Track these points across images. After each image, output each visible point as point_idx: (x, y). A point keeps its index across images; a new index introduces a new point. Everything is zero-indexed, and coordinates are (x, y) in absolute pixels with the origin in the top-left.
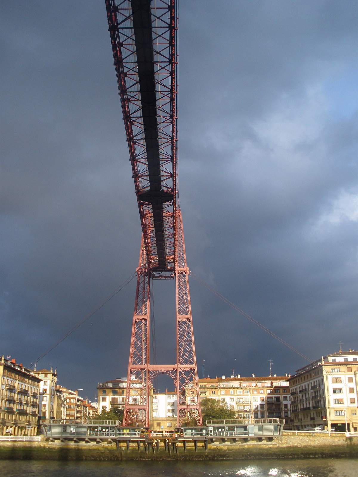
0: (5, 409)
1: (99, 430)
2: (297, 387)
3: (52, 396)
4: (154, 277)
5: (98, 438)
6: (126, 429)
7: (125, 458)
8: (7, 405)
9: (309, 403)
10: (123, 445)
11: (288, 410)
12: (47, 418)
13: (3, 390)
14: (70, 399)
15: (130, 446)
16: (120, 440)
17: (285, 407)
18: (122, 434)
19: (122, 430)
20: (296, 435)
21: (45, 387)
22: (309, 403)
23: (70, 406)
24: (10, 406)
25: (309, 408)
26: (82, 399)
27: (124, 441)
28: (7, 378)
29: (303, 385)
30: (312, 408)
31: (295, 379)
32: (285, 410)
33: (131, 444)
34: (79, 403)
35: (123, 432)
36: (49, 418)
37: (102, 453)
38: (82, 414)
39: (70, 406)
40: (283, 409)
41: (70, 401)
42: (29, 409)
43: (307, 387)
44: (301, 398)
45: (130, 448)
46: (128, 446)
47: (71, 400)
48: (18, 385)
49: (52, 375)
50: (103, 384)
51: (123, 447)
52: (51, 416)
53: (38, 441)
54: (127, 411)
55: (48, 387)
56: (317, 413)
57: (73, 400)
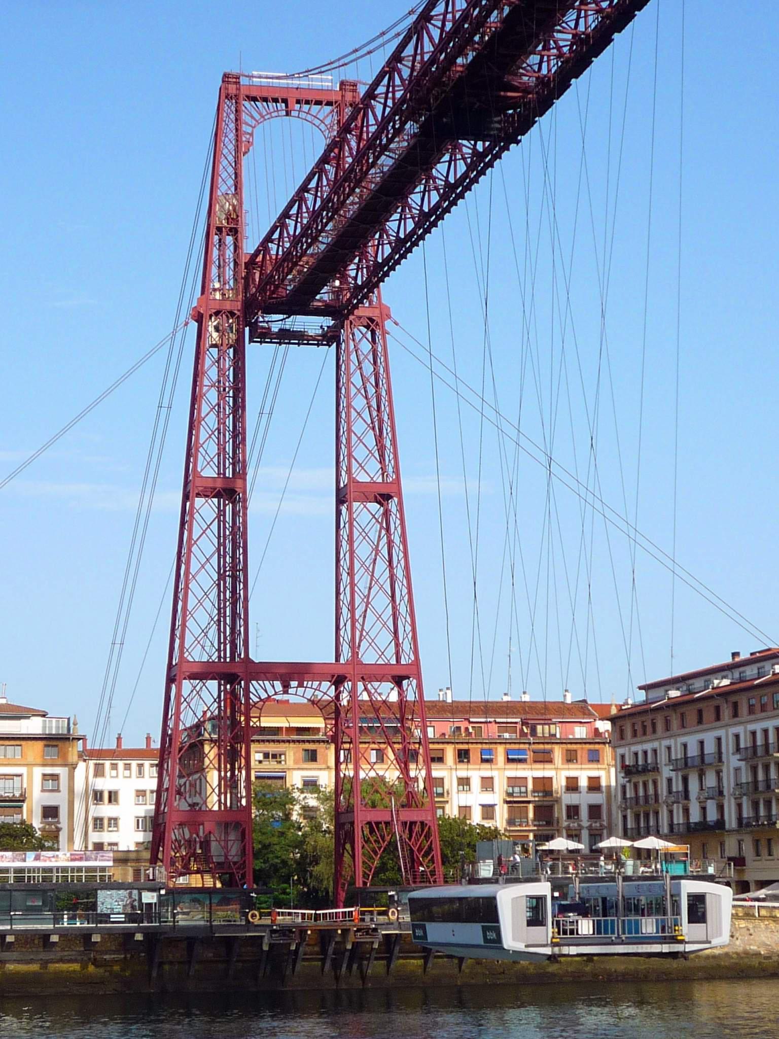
2: (656, 744)
4: (263, 335)
9: (721, 808)
11: (580, 828)
17: (569, 817)
20: (754, 916)
22: (721, 808)
25: (720, 824)
29: (692, 741)
30: (731, 821)
31: (648, 719)
32: (591, 825)
40: (565, 824)
43: (710, 748)
44: (678, 786)
56: (757, 843)
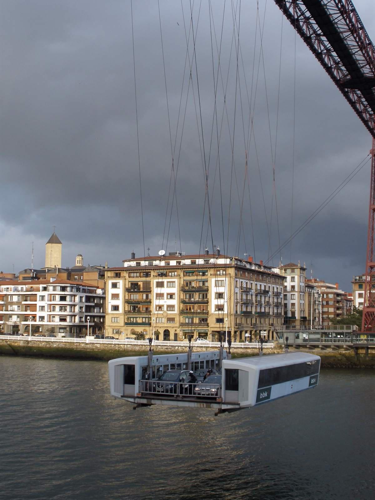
0: (241, 313)
1: (333, 336)
3: (301, 293)
5: (332, 344)
6: (364, 334)
7: (364, 366)
8: (244, 309)
10: (362, 352)
12: (297, 318)
13: (237, 293)
14: (327, 294)
15: (369, 352)
16: (358, 347)
18: (359, 341)
19: (359, 335)
21: (293, 284)
23: (327, 303)
24: (248, 310)
26: (343, 293)
27: (362, 348)
28: (241, 280)
33: (370, 351)
34: (339, 298)
35: (360, 338)
36: (299, 318)
37: (339, 360)
38: (345, 310)
39: (327, 303)
41: (328, 297)
42: (272, 311)
45: (369, 355)
46: (367, 353)
47: (329, 295)
48: (257, 285)
49: (299, 269)
50: (359, 277)
51: (362, 354)
52: (302, 316)
53: (271, 348)
54: (365, 314)
55: (296, 284)
57: (331, 295)
